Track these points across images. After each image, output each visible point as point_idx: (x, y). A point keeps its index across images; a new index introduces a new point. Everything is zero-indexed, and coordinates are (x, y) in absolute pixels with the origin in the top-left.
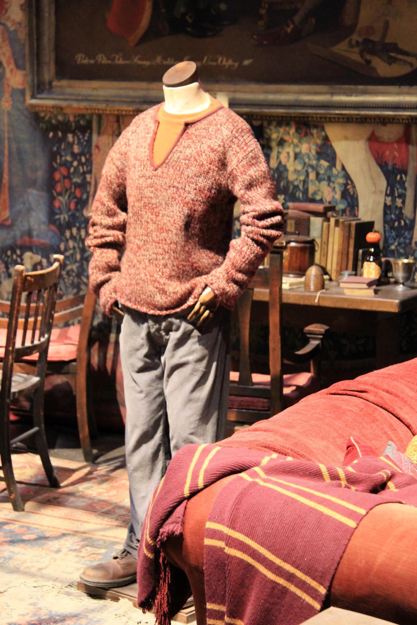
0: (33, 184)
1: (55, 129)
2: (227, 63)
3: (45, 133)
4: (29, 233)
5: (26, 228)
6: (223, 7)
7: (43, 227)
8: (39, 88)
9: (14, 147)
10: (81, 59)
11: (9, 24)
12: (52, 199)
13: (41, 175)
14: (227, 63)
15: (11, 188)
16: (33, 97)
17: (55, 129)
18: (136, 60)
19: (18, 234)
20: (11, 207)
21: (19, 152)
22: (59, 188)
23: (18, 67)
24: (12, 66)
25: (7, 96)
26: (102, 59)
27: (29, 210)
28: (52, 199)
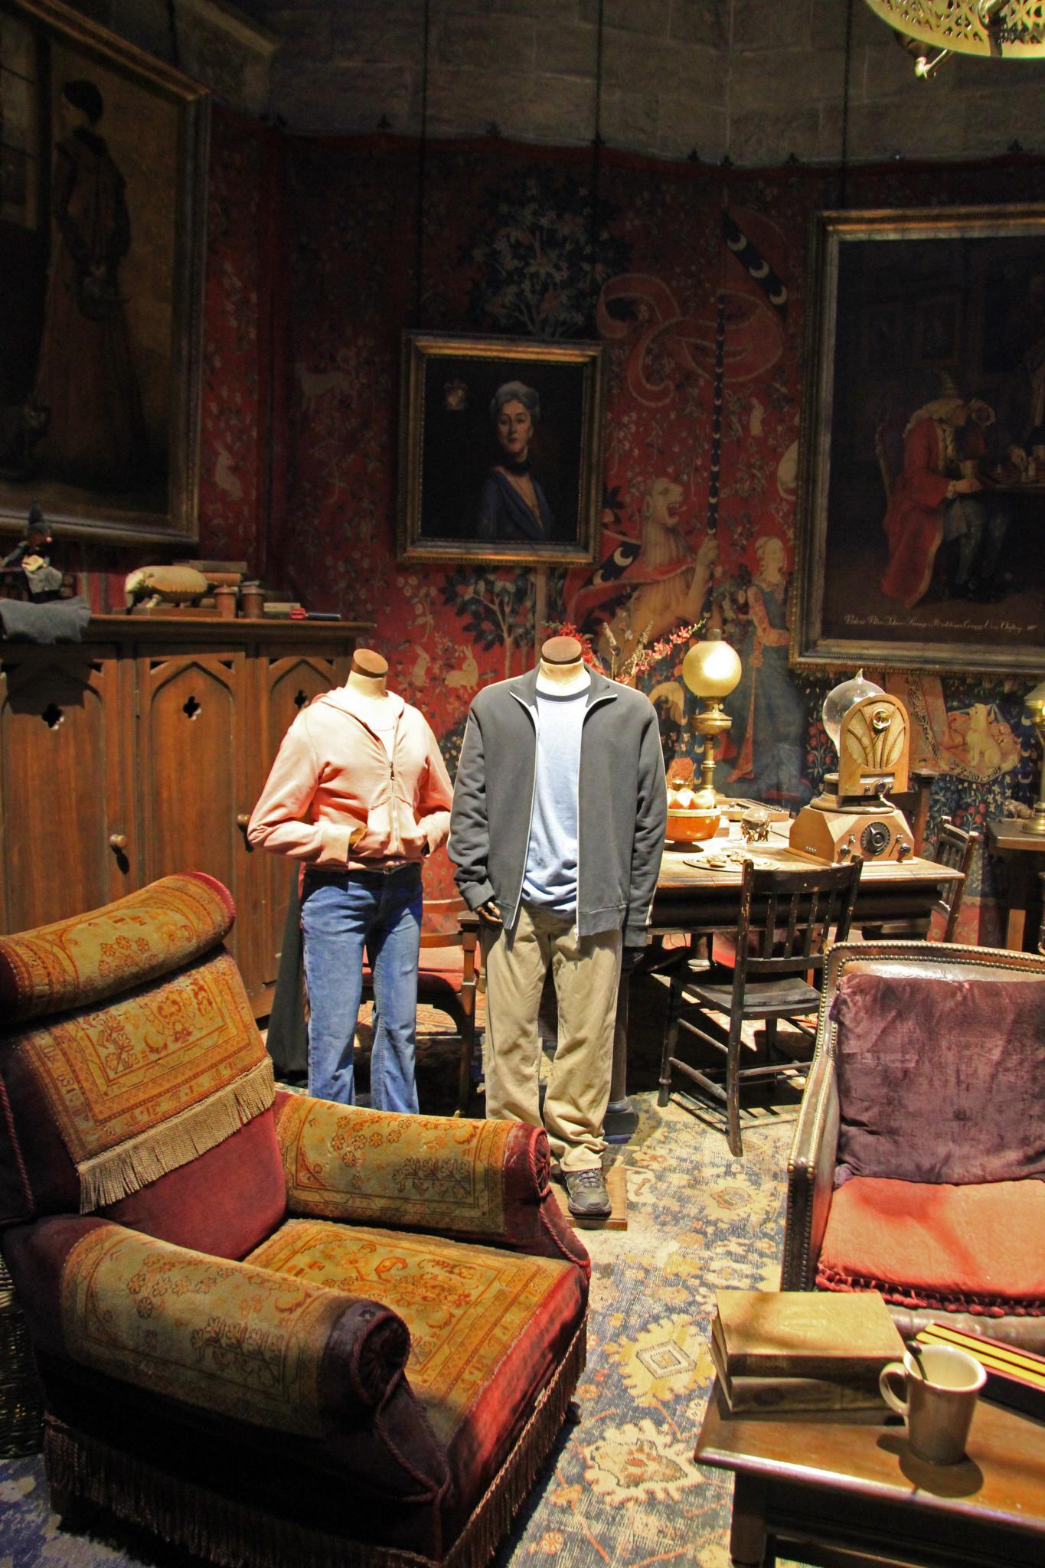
0: (784, 738)
1: (812, 685)
2: (1009, 627)
3: (800, 690)
4: (778, 787)
5: (775, 781)
6: (1008, 576)
7: (794, 781)
8: (807, 647)
9: (762, 702)
10: (850, 619)
11: (764, 586)
12: (805, 753)
13: (794, 730)
14: (1009, 627)
15: (755, 742)
16: (801, 655)
17: (812, 685)
18: (912, 622)
19: (763, 787)
20: (755, 761)
21: (769, 707)
22: (814, 743)
23: (772, 625)
24: (766, 625)
25: (757, 653)
26: (874, 620)
27: (779, 764)
28: (805, 753)
